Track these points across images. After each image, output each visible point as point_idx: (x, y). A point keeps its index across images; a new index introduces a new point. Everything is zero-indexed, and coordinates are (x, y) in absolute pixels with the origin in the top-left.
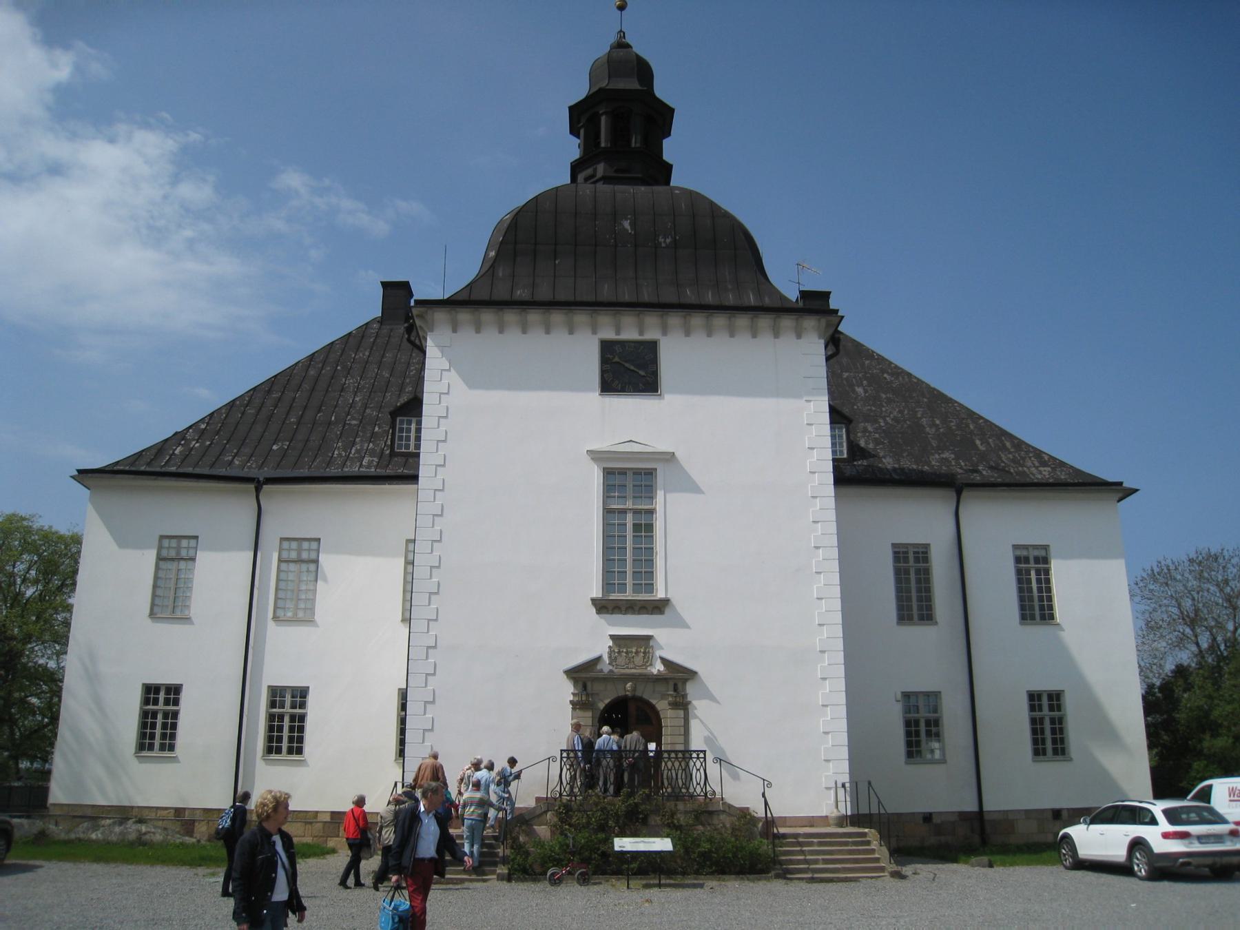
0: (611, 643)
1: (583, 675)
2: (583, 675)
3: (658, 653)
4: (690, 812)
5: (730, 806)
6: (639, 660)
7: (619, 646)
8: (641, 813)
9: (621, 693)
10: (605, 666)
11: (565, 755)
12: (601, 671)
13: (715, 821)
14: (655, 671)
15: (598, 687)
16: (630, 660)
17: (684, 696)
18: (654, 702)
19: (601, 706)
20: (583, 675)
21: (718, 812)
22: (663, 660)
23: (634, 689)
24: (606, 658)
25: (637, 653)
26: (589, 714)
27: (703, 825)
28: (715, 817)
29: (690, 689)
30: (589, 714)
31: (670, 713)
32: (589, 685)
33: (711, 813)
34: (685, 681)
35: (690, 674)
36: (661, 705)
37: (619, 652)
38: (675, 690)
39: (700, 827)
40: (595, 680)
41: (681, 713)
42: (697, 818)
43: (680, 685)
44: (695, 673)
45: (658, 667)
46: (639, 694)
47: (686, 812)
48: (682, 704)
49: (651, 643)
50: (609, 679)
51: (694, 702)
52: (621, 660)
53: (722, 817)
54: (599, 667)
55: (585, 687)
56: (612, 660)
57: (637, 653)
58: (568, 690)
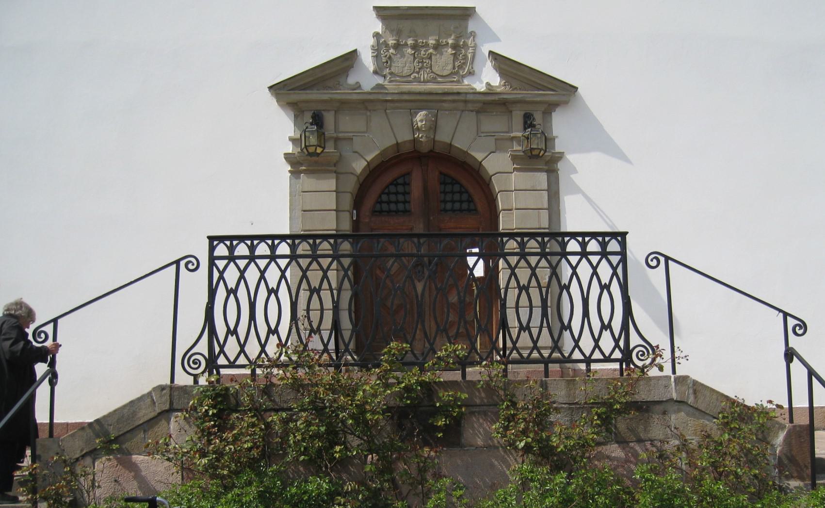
0: (378, 27)
1: (314, 95)
2: (315, 97)
3: (485, 49)
4: (588, 407)
5: (698, 388)
6: (443, 62)
7: (399, 33)
8: (443, 410)
9: (404, 136)
10: (366, 77)
11: (222, 250)
12: (358, 86)
13: (657, 431)
14: (480, 87)
15: (349, 124)
16: (424, 63)
17: (548, 140)
18: (479, 156)
19: (359, 166)
20: (315, 97)
21: (663, 406)
22: (501, 62)
23: (434, 127)
24: (367, 59)
25: (438, 47)
26: (330, 183)
27: (622, 442)
28: (656, 420)
29: (562, 128)
30: (330, 183)
31: (517, 179)
32: (329, 119)
33: (644, 408)
34: (550, 108)
35: (561, 93)
36: (496, 164)
37: (397, 46)
38: (528, 122)
39: (615, 451)
40: (342, 106)
41: (541, 179)
42: (606, 421)
43: (538, 118)
44: (573, 89)
45: (487, 78)
46: (444, 136)
47: (574, 407)
48: (541, 158)
49: (472, 26)
50: (369, 104)
51: (571, 157)
52: (403, 64)
53: (676, 418)
54: (352, 80)
55: (318, 120)
56: (383, 63)
57: (438, 47)
58: (281, 130)
